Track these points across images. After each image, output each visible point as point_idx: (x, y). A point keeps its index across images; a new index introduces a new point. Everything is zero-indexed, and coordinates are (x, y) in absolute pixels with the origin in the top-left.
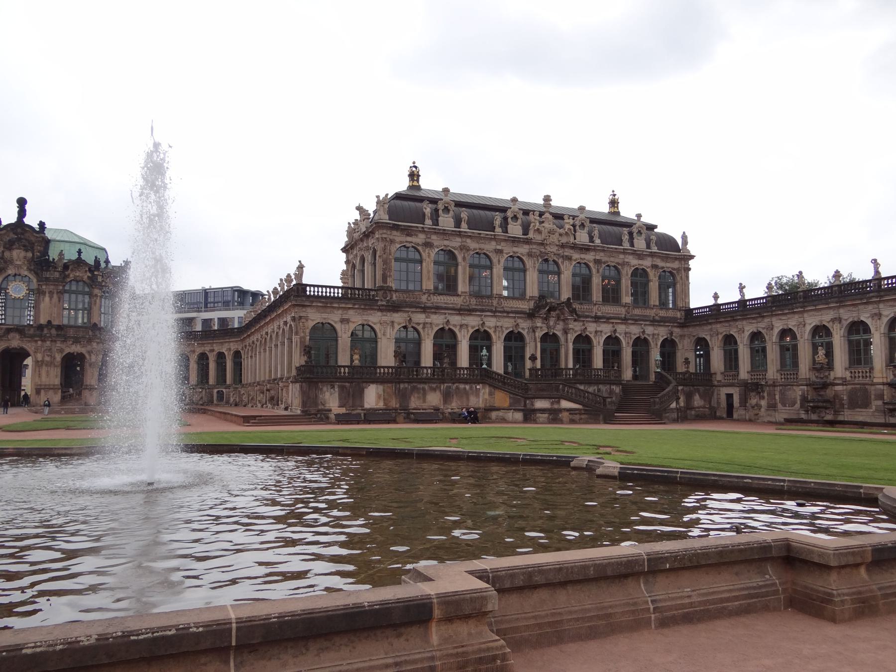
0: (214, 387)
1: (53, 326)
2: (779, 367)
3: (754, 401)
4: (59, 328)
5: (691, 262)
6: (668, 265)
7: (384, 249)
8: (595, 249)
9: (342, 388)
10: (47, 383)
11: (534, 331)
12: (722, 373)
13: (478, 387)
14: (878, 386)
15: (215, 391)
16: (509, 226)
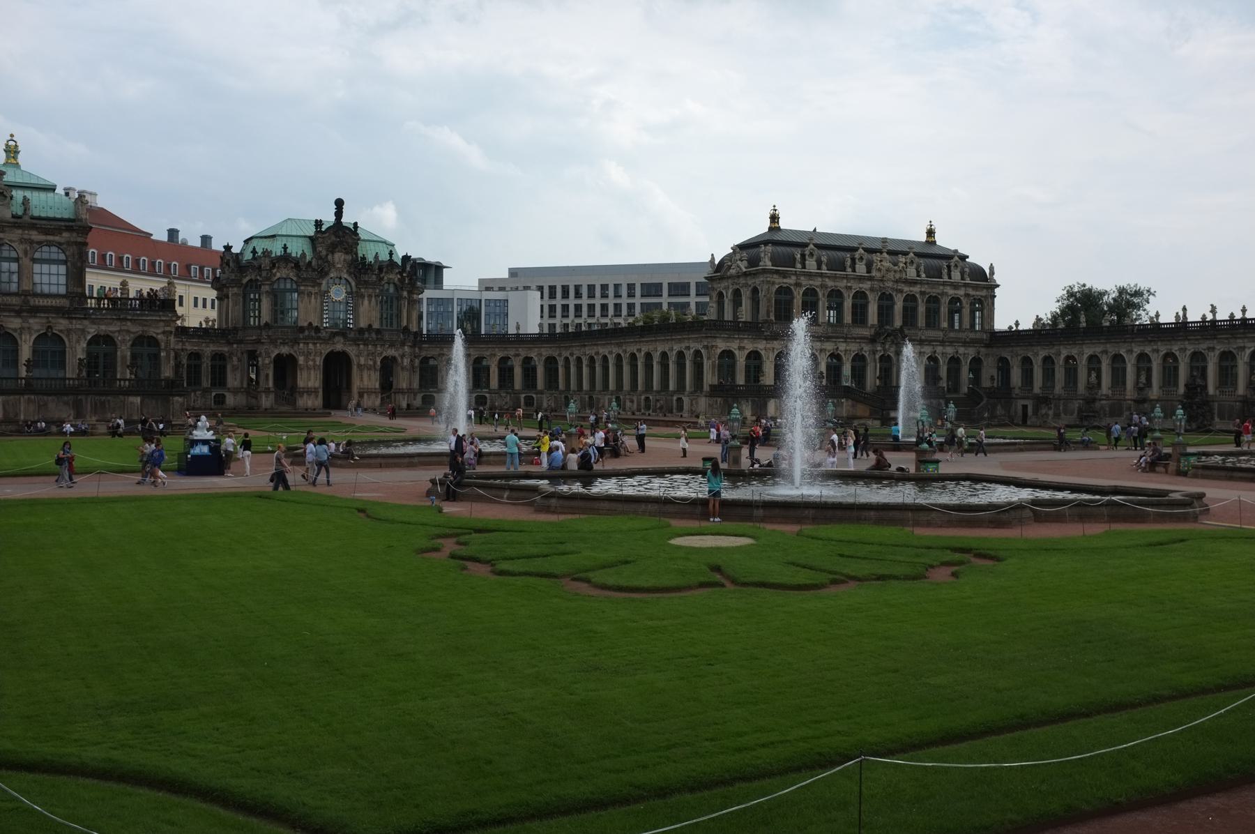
0: (519, 392)
1: (373, 330)
2: (1063, 385)
3: (1044, 411)
4: (378, 331)
5: (996, 290)
6: (978, 293)
7: (768, 289)
8: (921, 283)
9: (753, 402)
10: (370, 387)
11: (874, 354)
12: (1019, 388)
13: (842, 401)
14: (1128, 402)
15: (523, 395)
16: (857, 266)
